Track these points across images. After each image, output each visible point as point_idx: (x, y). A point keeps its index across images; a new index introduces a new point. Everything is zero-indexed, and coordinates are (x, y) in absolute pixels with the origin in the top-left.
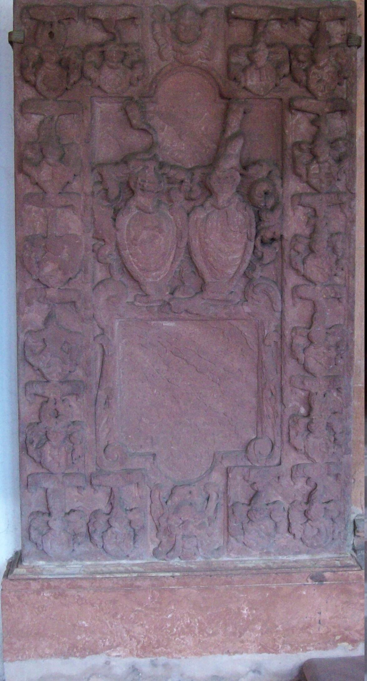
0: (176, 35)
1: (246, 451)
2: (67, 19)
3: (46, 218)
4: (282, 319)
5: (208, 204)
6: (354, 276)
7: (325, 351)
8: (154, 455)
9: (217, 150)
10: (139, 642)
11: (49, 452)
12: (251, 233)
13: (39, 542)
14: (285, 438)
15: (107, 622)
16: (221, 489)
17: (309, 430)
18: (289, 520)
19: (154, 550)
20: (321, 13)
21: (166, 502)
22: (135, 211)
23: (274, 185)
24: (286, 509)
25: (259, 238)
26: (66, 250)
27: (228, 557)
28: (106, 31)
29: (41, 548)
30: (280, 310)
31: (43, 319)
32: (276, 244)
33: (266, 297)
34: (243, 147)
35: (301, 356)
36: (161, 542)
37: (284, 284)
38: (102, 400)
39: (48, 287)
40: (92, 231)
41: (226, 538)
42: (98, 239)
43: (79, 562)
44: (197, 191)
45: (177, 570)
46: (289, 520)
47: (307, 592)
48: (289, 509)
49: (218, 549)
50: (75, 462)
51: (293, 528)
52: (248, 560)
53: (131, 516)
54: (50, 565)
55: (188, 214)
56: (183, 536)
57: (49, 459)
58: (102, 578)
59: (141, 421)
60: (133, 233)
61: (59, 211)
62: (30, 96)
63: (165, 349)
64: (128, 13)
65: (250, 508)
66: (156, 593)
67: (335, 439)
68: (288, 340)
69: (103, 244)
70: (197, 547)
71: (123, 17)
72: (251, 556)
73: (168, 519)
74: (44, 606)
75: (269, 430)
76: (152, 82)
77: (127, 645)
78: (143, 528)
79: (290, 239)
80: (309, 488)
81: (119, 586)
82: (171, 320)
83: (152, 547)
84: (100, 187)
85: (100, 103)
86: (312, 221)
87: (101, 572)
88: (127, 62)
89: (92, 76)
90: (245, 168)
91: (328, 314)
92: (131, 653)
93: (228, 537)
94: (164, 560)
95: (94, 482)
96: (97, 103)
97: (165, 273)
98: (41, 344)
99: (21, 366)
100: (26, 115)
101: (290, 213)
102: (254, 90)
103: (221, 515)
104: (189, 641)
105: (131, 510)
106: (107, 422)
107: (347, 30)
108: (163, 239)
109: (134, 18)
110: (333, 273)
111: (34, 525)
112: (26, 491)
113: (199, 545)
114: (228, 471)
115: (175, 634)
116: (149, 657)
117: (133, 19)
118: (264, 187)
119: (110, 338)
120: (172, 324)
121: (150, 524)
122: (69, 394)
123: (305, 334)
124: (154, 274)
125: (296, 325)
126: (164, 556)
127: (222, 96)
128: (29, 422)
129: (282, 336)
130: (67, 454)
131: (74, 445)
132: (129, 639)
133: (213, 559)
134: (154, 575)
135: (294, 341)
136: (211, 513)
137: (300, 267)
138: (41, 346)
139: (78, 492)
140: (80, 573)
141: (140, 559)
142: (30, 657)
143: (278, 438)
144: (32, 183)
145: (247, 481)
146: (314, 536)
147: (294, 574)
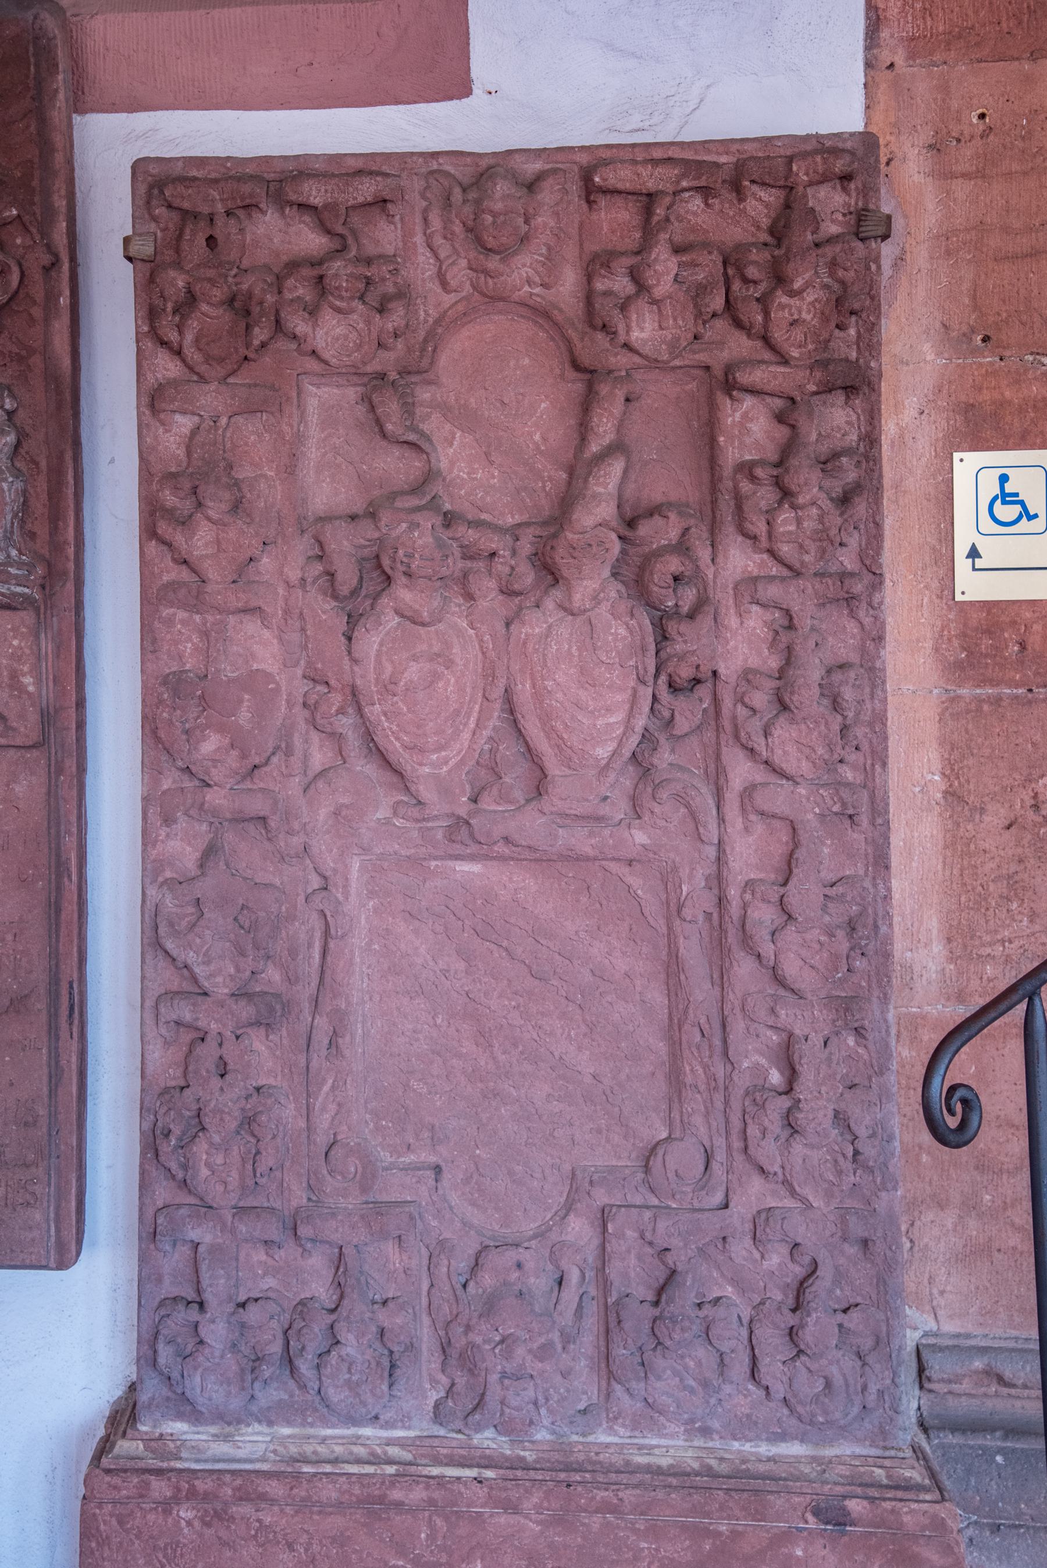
0: (474, 231)
1: (647, 1168)
2: (244, 207)
3: (205, 634)
4: (720, 860)
5: (549, 604)
7: (822, 938)
8: (438, 1169)
9: (569, 484)
11: (204, 1157)
12: (645, 670)
13: (175, 1375)
14: (737, 1144)
16: (590, 1260)
17: (791, 1126)
18: (753, 1349)
19: (437, 1406)
20: (795, 168)
21: (465, 1286)
22: (392, 621)
23: (695, 561)
24: (745, 1321)
26: (246, 704)
27: (610, 1435)
28: (328, 232)
29: (179, 1391)
30: (716, 842)
31: (198, 855)
32: (704, 691)
33: (683, 810)
34: (625, 471)
35: (768, 950)
36: (453, 1385)
37: (722, 780)
38: (321, 1039)
39: (208, 785)
40: (302, 662)
41: (604, 1383)
44: (528, 576)
45: (488, 1463)
47: (805, 1550)
48: (751, 1321)
49: (584, 1412)
50: (262, 1181)
51: (763, 1370)
52: (658, 1446)
53: (383, 1317)
54: (198, 1433)
55: (508, 625)
56: (504, 1375)
57: (204, 1172)
58: (315, 1475)
59: (406, 1087)
60: (389, 669)
61: (232, 619)
62: (171, 375)
63: (460, 923)
64: (372, 189)
65: (656, 1312)
66: (439, 1522)
67: (856, 1153)
69: (326, 691)
70: (535, 1403)
73: (468, 1328)
74: (178, 1542)
75: (698, 1120)
76: (426, 341)
78: (411, 1347)
79: (733, 680)
80: (798, 1271)
81: (354, 1499)
82: (472, 858)
83: (433, 1396)
84: (318, 568)
86: (784, 638)
87: (314, 1458)
88: (372, 298)
90: (631, 523)
93: (609, 1384)
94: (460, 1431)
95: (304, 1231)
96: (310, 387)
97: (459, 753)
98: (191, 910)
99: (149, 957)
100: (162, 416)
101: (733, 621)
102: (646, 350)
103: (591, 1322)
105: (385, 1303)
106: (333, 1088)
107: (856, 204)
108: (453, 680)
109: (385, 201)
110: (836, 757)
111: (164, 1332)
112: (152, 1246)
113: (541, 1400)
114: (603, 1218)
117: (382, 203)
118: (674, 564)
119: (340, 896)
120: (475, 868)
122: (251, 1025)
123: (775, 898)
124: (434, 757)
125: (752, 876)
126: (459, 1424)
127: (576, 366)
128: (163, 1085)
129: (721, 901)
131: (258, 1141)
133: (575, 1438)
135: (749, 912)
136: (566, 1317)
137: (759, 743)
138: (193, 914)
139: (267, 1254)
141: (404, 1427)
143: (720, 1142)
144: (174, 560)
145: (651, 1243)
146: (817, 1396)
147: (770, 1497)
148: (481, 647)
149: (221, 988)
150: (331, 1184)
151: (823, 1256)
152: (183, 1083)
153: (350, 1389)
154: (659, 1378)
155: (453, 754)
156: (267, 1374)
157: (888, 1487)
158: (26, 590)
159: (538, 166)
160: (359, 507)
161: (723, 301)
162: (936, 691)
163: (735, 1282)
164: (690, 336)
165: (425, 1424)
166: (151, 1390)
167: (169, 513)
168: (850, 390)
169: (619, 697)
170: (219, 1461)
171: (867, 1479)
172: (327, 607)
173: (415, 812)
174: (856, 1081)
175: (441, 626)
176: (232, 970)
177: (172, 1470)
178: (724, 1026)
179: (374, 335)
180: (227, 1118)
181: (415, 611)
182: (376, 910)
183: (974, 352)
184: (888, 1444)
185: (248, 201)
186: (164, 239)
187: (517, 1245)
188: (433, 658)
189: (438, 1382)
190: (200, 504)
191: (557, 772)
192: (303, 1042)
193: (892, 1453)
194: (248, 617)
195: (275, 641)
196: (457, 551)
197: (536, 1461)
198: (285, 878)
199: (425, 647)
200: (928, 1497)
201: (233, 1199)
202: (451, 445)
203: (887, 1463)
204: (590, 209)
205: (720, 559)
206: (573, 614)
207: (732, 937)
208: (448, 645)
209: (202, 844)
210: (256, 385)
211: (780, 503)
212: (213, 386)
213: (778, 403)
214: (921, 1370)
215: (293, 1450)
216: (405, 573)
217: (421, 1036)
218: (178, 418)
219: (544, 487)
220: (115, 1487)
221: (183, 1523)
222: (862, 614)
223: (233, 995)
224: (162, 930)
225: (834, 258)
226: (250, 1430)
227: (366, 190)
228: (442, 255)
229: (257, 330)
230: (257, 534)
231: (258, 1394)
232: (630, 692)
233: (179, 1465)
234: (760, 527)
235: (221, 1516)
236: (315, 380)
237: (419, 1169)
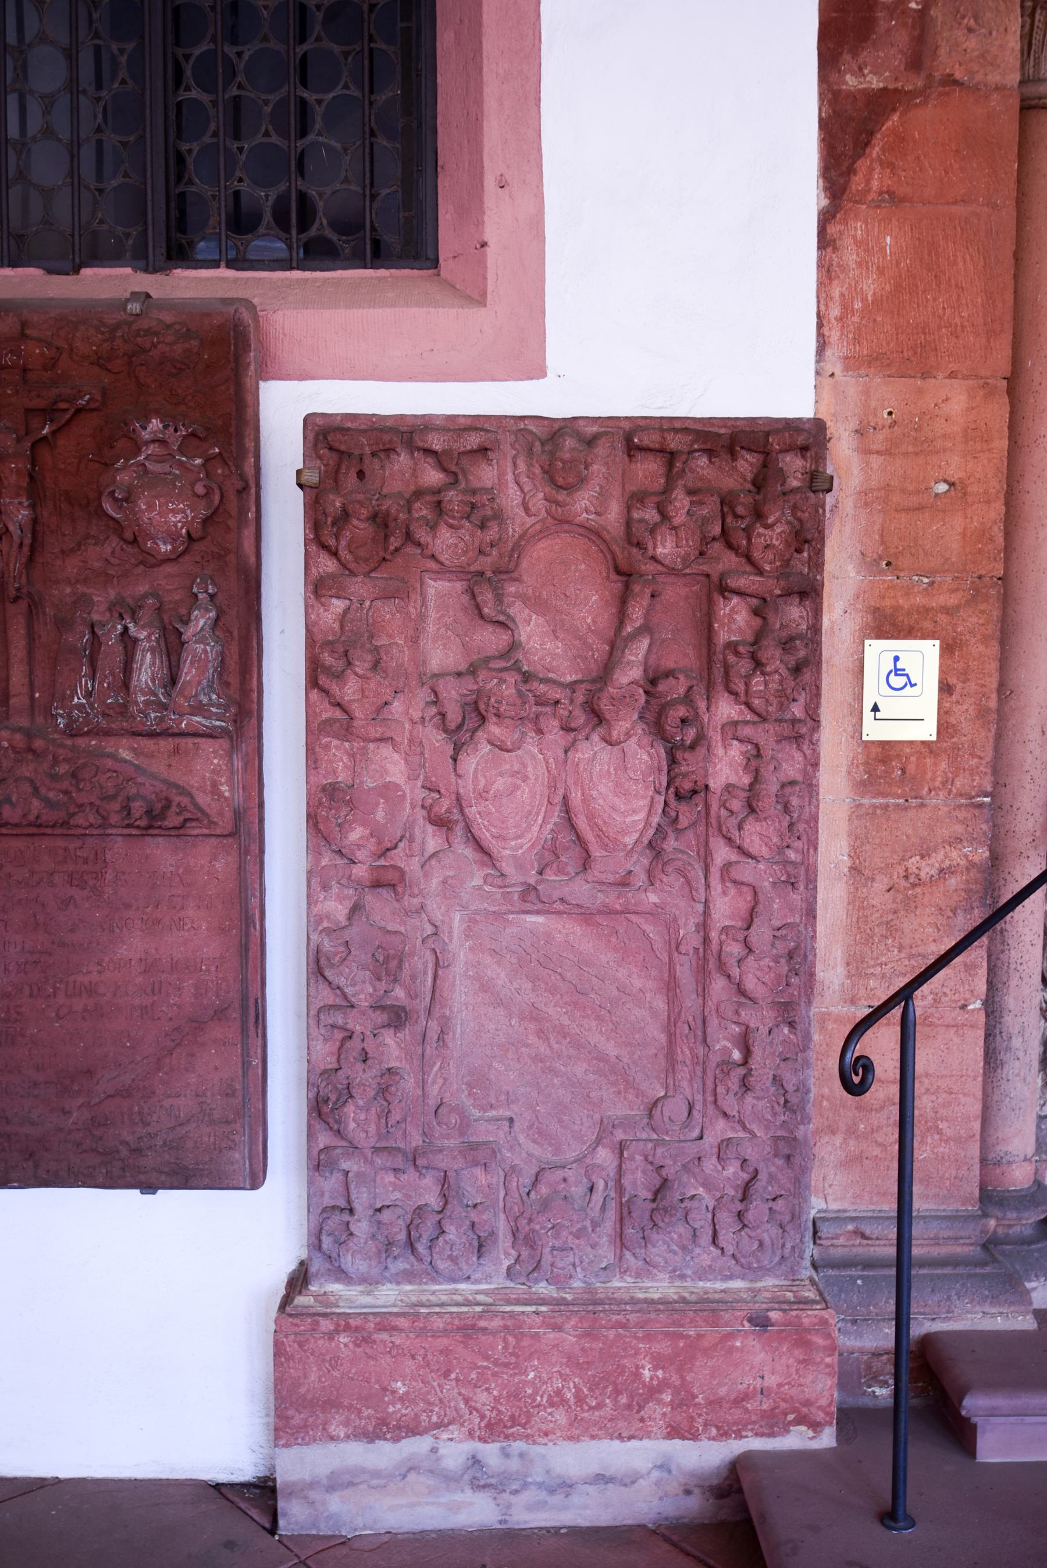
1: (650, 1116)
2: (385, 450)
3: (352, 756)
4: (706, 913)
5: (595, 737)
6: (816, 849)
7: (771, 964)
8: (511, 1120)
9: (611, 653)
10: (482, 1417)
13: (334, 1255)
14: (710, 1098)
15: (435, 1384)
16: (612, 1174)
17: (745, 1085)
18: (714, 1225)
19: (509, 1269)
21: (528, 1194)
23: (696, 710)
24: (711, 1209)
25: (672, 790)
28: (445, 470)
29: (337, 1265)
31: (347, 911)
32: (699, 799)
33: (682, 880)
35: (735, 972)
36: (519, 1256)
37: (709, 860)
38: (433, 1034)
39: (354, 863)
40: (421, 777)
41: (618, 1251)
42: (430, 789)
43: (394, 1286)
44: (580, 718)
45: (542, 1302)
46: (714, 1225)
49: (605, 1269)
50: (392, 1130)
51: (721, 1238)
53: (473, 1215)
55: (566, 752)
56: (553, 1248)
57: (352, 1125)
58: (429, 1314)
59: (490, 1067)
60: (482, 783)
61: (371, 746)
64: (477, 441)
65: (654, 1206)
66: (511, 1339)
67: (786, 1101)
68: (714, 946)
70: (574, 1265)
71: (469, 447)
72: (656, 1281)
73: (530, 1220)
74: (338, 1357)
75: (685, 1084)
76: (513, 550)
77: (464, 1421)
78: (492, 1234)
79: (719, 791)
80: (746, 1176)
82: (538, 912)
83: (506, 1263)
84: (434, 710)
85: (435, 580)
88: (476, 518)
89: (422, 540)
90: (653, 682)
91: (775, 906)
92: (471, 1434)
93: (621, 1251)
94: (524, 1284)
95: (419, 1162)
98: (342, 949)
99: (312, 981)
100: (323, 600)
101: (720, 751)
103: (611, 1214)
104: (560, 1417)
105: (475, 1206)
106: (441, 1068)
109: (486, 449)
110: (785, 844)
111: (327, 1228)
112: (317, 1174)
113: (578, 1263)
114: (621, 1147)
115: (539, 1405)
116: (499, 1441)
117: (483, 451)
118: (682, 711)
119: (447, 941)
120: (540, 919)
121: (502, 1227)
123: (741, 937)
124: (513, 843)
126: (523, 1280)
127: (618, 572)
128: (323, 1068)
129: (706, 941)
130: (379, 1117)
132: (467, 1412)
133: (599, 1285)
134: (508, 1309)
136: (595, 1212)
137: (735, 834)
140: (394, 1305)
141: (487, 1283)
142: (315, 1440)
143: (699, 1097)
144: (331, 704)
145: (651, 1163)
146: (754, 1252)
148: (547, 767)
149: (363, 1000)
150: (438, 1130)
151: (761, 1167)
152: (335, 1066)
153: (452, 1260)
154: (654, 1246)
155: (526, 841)
156: (396, 1253)
157: (794, 1303)
158: (223, 724)
159: (594, 429)
160: (463, 667)
161: (720, 530)
162: (847, 800)
163: (704, 1185)
164: (697, 553)
165: (501, 1281)
166: (317, 1265)
167: (328, 670)
168: (803, 595)
169: (642, 803)
170: (365, 1307)
171: (782, 1299)
172: (439, 737)
173: (499, 882)
174: (788, 1056)
175: (519, 752)
176: (371, 990)
177: (333, 1313)
178: (704, 1022)
179: (477, 544)
180: (368, 1089)
181: (502, 741)
182: (471, 949)
183: (881, 572)
184: (795, 1277)
185: (388, 446)
186: (326, 472)
187: (564, 1167)
188: (514, 774)
189: (509, 1254)
190: (349, 663)
191: (598, 854)
192: (420, 1038)
193: (798, 1283)
194: (383, 744)
195: (402, 762)
196: (532, 699)
197: (574, 1300)
198: (408, 927)
199: (508, 766)
200: (818, 1307)
201: (372, 1142)
202: (529, 624)
203: (794, 1289)
204: (631, 461)
205: (713, 708)
206: (611, 745)
207: (712, 965)
208: (524, 765)
209: (349, 904)
210: (391, 579)
211: (754, 670)
212: (360, 579)
213: (755, 602)
214: (815, 1233)
215: (414, 1299)
216: (495, 714)
217: (500, 1033)
218: (334, 601)
219: (593, 655)
220: (296, 1325)
221: (342, 1346)
222: (805, 747)
223: (371, 1007)
224: (323, 962)
225: (795, 504)
226: (384, 1287)
227: (473, 441)
228: (526, 490)
229: (392, 539)
230: (391, 685)
231: (390, 1266)
232: (649, 799)
233: (338, 1310)
234: (741, 688)
235: (367, 1340)
236: (433, 576)
237: (498, 1120)
